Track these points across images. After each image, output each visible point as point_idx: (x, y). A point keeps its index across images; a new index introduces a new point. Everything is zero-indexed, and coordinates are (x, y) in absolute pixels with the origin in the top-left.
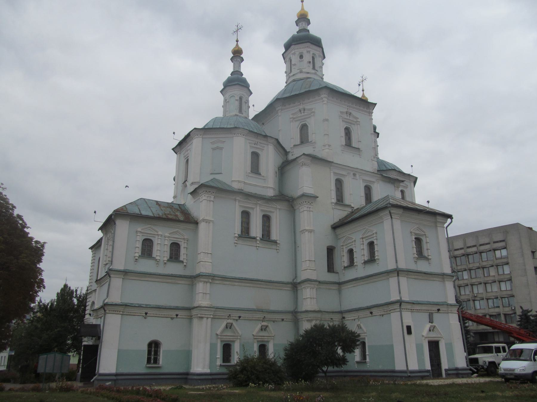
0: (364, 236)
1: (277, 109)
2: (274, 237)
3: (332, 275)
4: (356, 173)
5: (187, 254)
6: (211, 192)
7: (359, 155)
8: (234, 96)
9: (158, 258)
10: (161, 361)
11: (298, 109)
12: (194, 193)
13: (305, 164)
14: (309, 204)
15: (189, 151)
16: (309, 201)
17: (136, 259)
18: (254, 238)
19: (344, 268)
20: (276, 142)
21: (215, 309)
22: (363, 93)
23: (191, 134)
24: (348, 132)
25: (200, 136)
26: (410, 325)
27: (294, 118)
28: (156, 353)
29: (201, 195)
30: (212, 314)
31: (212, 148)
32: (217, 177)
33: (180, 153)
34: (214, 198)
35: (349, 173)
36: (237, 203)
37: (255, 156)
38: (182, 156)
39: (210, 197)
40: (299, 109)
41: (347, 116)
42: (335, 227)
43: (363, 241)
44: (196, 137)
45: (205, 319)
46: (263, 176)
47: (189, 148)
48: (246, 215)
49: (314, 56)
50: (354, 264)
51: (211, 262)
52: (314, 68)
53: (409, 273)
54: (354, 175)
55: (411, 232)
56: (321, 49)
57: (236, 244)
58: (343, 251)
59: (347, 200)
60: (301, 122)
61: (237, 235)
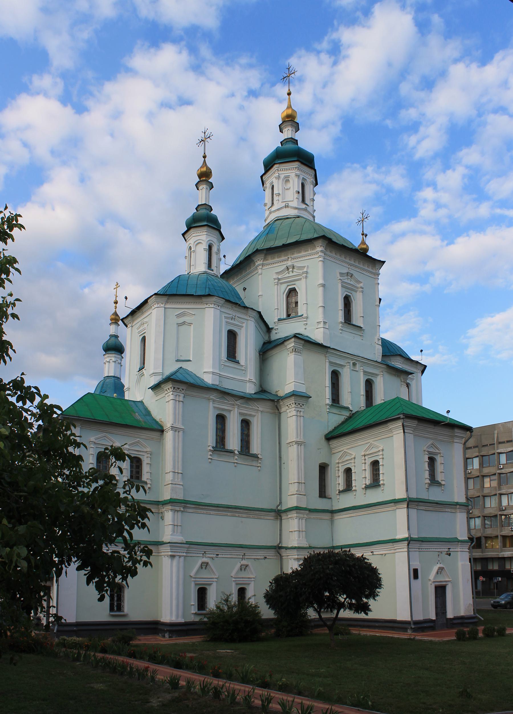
0: (367, 453)
1: (257, 264)
3: (324, 500)
4: (356, 362)
5: (151, 473)
6: (180, 389)
10: (127, 607)
11: (285, 266)
12: (156, 388)
14: (299, 406)
15: (146, 325)
19: (339, 492)
20: (257, 316)
21: (188, 545)
23: (149, 301)
24: (347, 302)
25: (162, 306)
26: (417, 568)
29: (166, 392)
30: (185, 551)
31: (177, 324)
32: (185, 365)
33: (132, 326)
37: (232, 336)
38: (136, 331)
39: (179, 396)
40: (287, 266)
42: (330, 437)
43: (365, 460)
44: (156, 306)
45: (177, 557)
46: (242, 366)
47: (145, 320)
48: (221, 419)
50: (353, 489)
51: (182, 485)
52: (303, 201)
53: (420, 503)
54: (354, 364)
56: (314, 172)
57: (210, 460)
58: (339, 470)
59: (346, 400)
60: (288, 286)
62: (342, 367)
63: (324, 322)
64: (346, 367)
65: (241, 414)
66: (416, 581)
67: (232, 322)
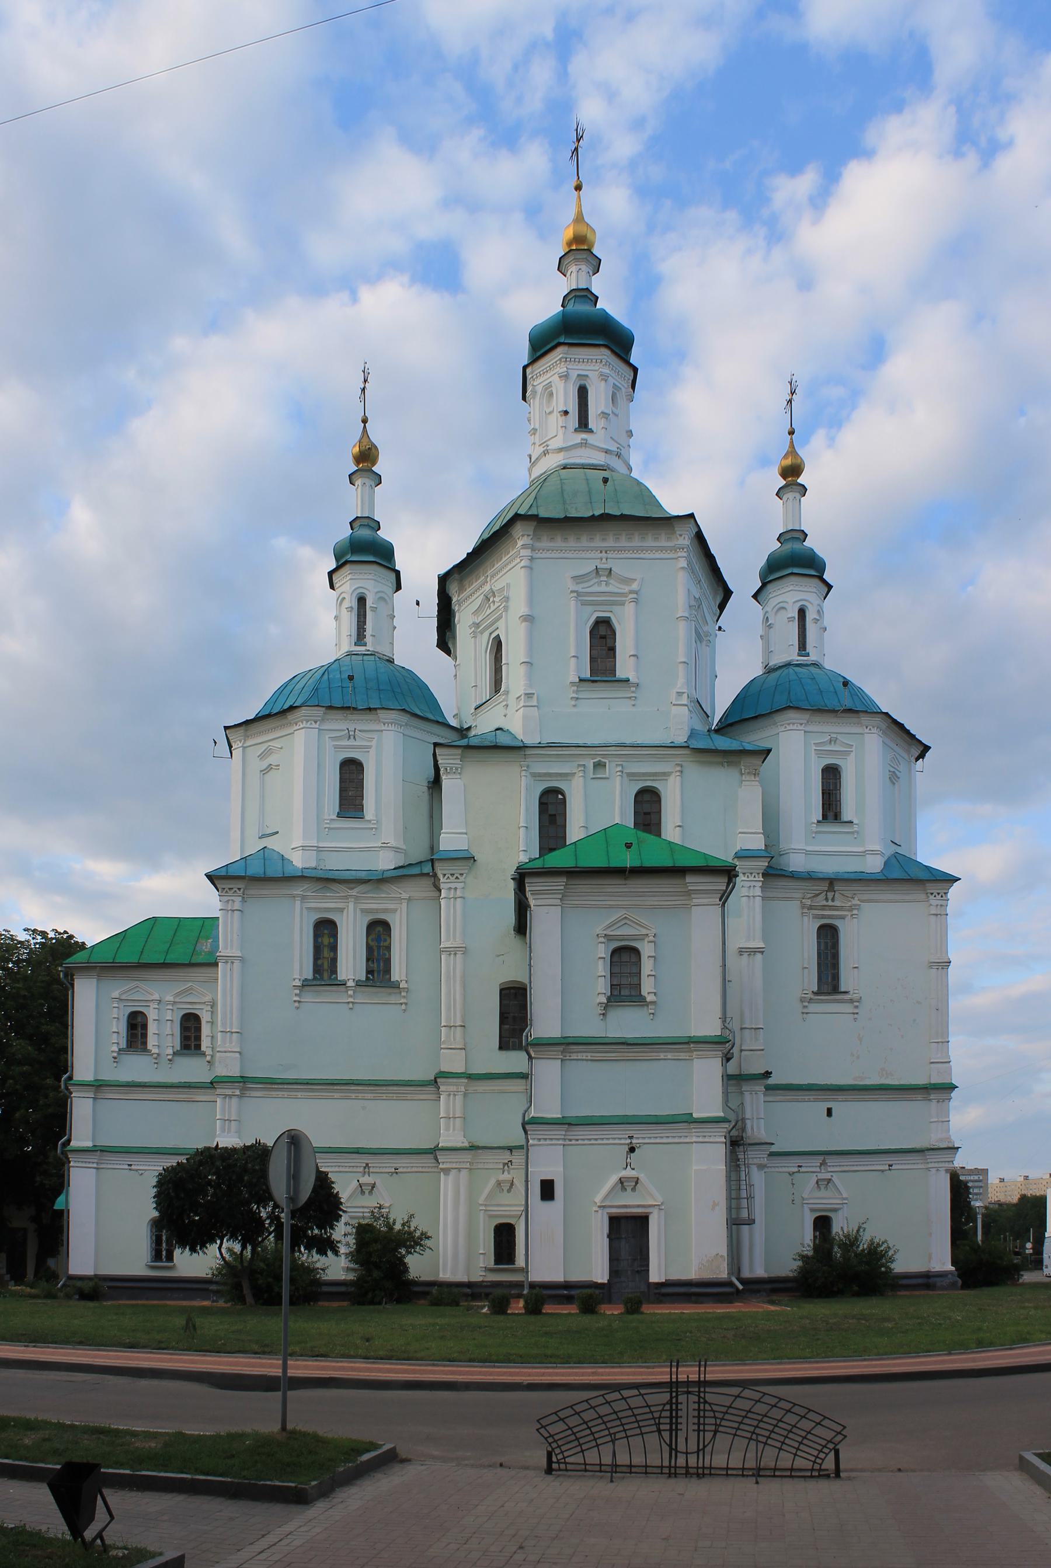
8: (344, 598)
14: (452, 879)
16: (452, 872)
27: (477, 625)
32: (272, 843)
34: (244, 901)
35: (579, 765)
46: (370, 821)
49: (582, 382)
60: (491, 634)
62: (569, 778)
64: (576, 776)
67: (352, 742)
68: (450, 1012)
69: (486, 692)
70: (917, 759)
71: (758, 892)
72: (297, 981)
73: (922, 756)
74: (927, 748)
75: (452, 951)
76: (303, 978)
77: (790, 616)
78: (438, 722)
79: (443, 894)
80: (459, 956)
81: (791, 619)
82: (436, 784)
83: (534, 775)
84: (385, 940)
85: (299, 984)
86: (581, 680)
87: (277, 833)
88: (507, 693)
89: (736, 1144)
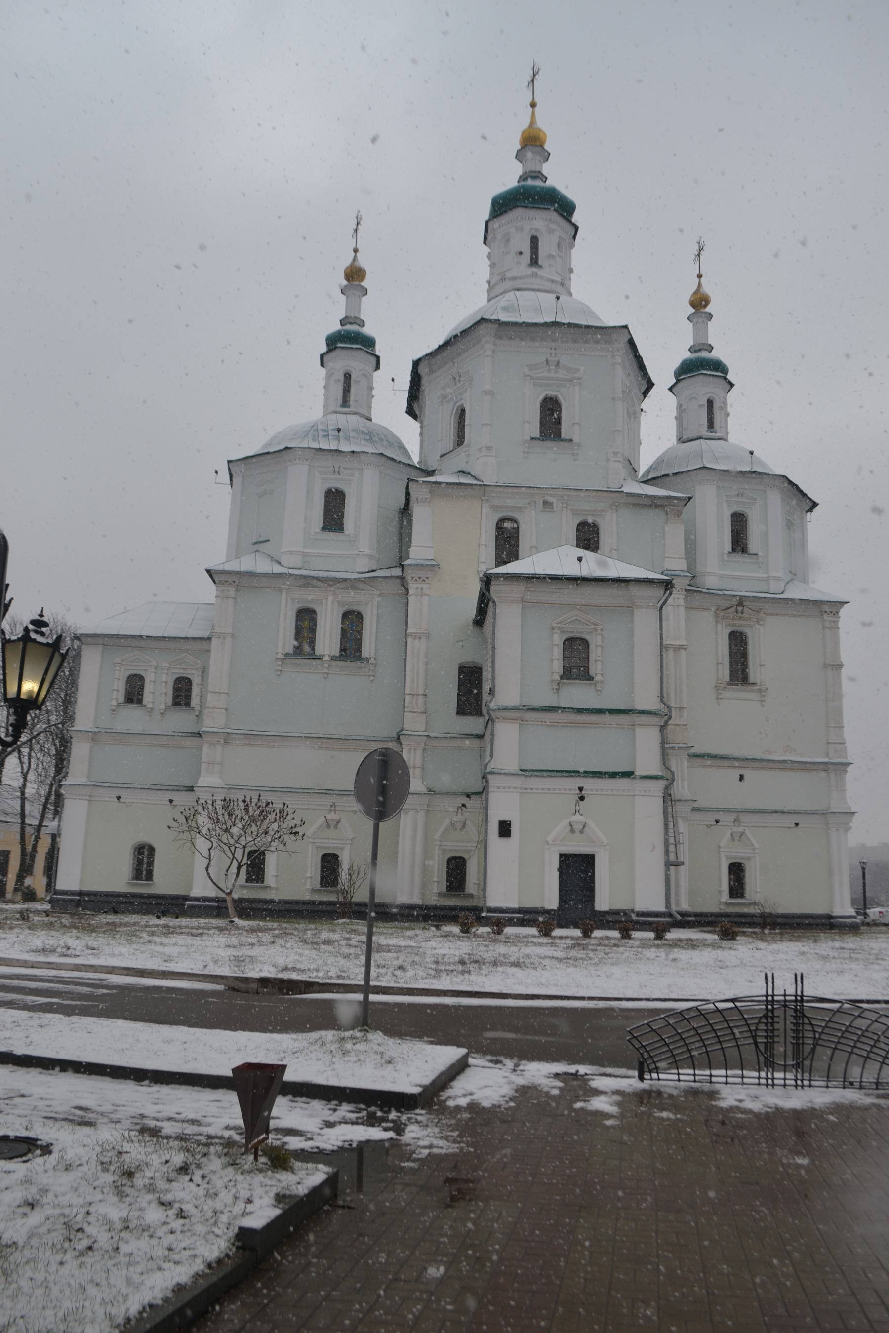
2: (366, 652)
7: (573, 454)
9: (150, 706)
13: (417, 499)
17: (114, 711)
18: (320, 658)
22: (700, 285)
28: (151, 864)
34: (237, 590)
36: (284, 594)
41: (549, 371)
46: (349, 535)
49: (534, 233)
55: (553, 628)
57: (278, 673)
60: (456, 403)
61: (280, 656)
63: (486, 447)
65: (340, 604)
66: (504, 841)
68: (414, 682)
69: (451, 446)
70: (807, 512)
71: (682, 602)
72: (280, 654)
73: (810, 510)
74: (815, 504)
75: (417, 636)
76: (285, 653)
77: (700, 403)
78: (409, 465)
79: (411, 592)
80: (423, 640)
81: (701, 406)
82: (406, 510)
83: (492, 507)
84: (357, 626)
85: (282, 657)
86: (532, 439)
87: (268, 540)
88: (469, 446)
89: (668, 798)
